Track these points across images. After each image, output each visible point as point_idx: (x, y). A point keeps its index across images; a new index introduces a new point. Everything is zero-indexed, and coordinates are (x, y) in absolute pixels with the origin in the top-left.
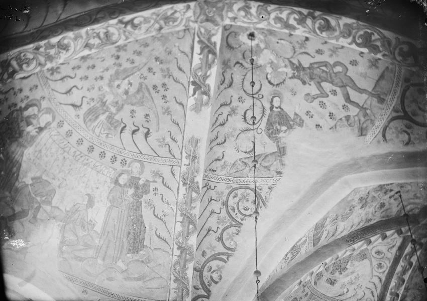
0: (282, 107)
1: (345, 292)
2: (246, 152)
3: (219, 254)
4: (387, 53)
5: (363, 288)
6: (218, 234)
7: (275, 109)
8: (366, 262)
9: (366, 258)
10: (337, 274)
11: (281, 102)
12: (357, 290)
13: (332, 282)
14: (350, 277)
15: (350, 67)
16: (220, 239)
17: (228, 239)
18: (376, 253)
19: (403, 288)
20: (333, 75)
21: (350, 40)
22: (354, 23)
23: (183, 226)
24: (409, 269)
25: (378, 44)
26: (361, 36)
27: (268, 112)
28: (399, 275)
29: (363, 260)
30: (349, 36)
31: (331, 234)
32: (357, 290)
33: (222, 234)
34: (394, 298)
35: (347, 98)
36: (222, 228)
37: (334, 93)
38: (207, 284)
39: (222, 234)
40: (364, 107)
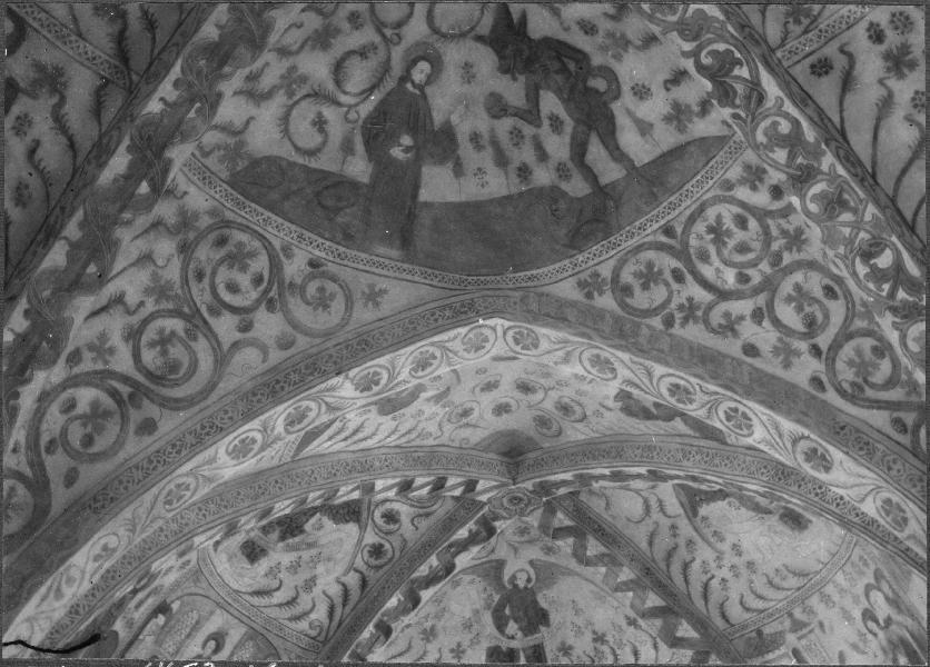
0: (428, 90)
2: (297, 149)
3: (112, 374)
4: (743, 115)
5: (317, 591)
6: (135, 320)
7: (409, 86)
8: (352, 528)
9: (358, 521)
10: (275, 535)
11: (430, 80)
14: (300, 553)
15: (628, 98)
16: (133, 335)
17: (152, 345)
18: (382, 517)
20: (581, 86)
21: (688, 47)
22: (717, 20)
23: (71, 257)
25: (739, 88)
26: (714, 53)
27: (390, 84)
29: (347, 521)
30: (694, 39)
33: (146, 322)
35: (579, 150)
36: (150, 307)
37: (556, 124)
38: (45, 439)
39: (146, 322)
40: (606, 190)
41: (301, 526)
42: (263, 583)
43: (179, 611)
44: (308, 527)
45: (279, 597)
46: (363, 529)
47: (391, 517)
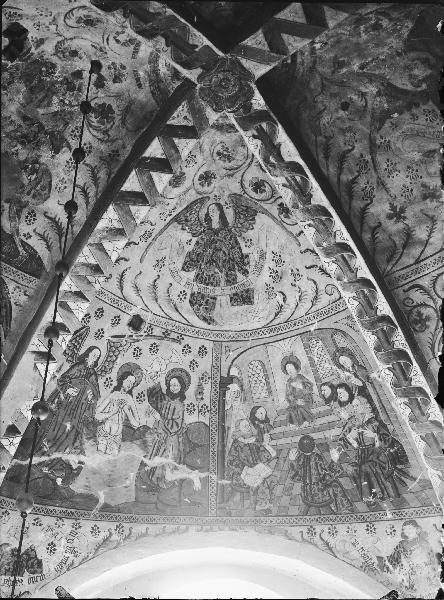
1: (282, 302)
5: (303, 271)
8: (261, 219)
9: (255, 213)
10: (240, 277)
12: (297, 283)
13: (244, 298)
14: (266, 268)
19: (338, 224)
24: (305, 181)
28: (301, 206)
29: (254, 219)
31: (52, 235)
32: (297, 283)
34: (343, 257)
44: (245, 251)
45: (292, 300)
47: (258, 186)
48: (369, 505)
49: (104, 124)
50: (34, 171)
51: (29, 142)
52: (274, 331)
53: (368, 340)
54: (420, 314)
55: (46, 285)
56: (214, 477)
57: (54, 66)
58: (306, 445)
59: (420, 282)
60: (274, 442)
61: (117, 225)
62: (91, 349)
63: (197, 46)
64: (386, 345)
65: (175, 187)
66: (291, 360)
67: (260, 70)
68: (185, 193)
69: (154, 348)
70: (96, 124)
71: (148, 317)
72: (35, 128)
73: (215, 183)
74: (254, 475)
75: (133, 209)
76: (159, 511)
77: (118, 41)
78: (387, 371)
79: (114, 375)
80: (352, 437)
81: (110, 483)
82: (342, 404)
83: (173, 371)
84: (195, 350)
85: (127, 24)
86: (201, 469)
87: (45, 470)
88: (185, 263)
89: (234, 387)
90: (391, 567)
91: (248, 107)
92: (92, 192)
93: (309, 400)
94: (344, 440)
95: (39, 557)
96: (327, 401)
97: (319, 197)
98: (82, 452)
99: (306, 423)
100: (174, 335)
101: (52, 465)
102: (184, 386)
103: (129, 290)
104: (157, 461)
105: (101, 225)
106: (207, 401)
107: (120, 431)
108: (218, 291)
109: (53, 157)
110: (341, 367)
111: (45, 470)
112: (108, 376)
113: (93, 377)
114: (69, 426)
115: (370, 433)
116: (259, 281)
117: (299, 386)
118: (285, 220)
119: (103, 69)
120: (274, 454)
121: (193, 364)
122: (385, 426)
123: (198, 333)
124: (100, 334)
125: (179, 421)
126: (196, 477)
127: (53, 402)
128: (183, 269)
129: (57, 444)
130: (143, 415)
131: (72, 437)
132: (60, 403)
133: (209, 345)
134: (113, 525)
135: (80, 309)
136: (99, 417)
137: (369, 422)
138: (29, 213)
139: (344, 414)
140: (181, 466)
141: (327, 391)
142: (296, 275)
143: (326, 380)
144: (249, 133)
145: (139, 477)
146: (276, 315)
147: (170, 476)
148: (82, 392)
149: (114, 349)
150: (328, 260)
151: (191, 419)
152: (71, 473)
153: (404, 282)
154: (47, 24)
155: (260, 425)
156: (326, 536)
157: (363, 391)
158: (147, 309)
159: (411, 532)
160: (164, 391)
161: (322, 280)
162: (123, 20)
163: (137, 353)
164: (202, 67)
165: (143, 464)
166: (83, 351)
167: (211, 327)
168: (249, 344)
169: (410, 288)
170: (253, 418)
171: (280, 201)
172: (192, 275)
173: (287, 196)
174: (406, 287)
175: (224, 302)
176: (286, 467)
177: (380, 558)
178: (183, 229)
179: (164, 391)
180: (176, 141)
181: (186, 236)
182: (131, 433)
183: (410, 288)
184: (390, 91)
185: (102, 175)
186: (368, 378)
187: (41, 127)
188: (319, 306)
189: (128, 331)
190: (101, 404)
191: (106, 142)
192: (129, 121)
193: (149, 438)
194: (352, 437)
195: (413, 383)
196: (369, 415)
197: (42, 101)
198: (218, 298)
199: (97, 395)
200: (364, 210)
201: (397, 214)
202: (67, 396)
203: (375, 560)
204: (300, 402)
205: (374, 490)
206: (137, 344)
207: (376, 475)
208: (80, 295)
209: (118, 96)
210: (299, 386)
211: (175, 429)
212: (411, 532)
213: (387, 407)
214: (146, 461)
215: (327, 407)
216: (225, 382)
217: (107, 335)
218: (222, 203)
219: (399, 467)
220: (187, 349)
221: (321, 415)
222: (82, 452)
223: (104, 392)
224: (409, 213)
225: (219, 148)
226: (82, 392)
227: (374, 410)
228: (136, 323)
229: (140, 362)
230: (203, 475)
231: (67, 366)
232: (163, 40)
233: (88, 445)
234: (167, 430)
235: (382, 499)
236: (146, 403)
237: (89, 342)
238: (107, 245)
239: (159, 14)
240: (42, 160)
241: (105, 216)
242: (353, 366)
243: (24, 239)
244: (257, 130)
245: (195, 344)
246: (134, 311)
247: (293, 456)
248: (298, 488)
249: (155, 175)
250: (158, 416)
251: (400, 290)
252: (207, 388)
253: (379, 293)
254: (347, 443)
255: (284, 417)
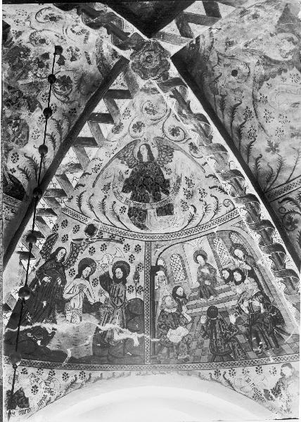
1: (193, 213)
5: (208, 191)
8: (177, 154)
9: (173, 150)
10: (163, 195)
12: (203, 199)
13: (167, 210)
14: (181, 189)
19: (231, 156)
24: (208, 126)
28: (205, 145)
29: (172, 155)
31: (30, 169)
32: (203, 199)
34: (235, 179)
41: (165, 180)
42: (187, 215)
43: (165, 263)
44: (166, 177)
45: (200, 211)
46: (180, 149)
47: (174, 131)
48: (257, 353)
49: (65, 90)
50: (16, 125)
51: (13, 104)
52: (187, 233)
53: (254, 237)
54: (290, 218)
55: (27, 205)
56: (148, 337)
57: (28, 50)
58: (212, 312)
59: (290, 196)
60: (190, 311)
61: (76, 161)
62: (59, 249)
63: (129, 34)
64: (267, 241)
65: (116, 133)
66: (200, 253)
67: (173, 49)
68: (124, 137)
69: (104, 248)
70: (59, 91)
71: (99, 226)
72: (16, 95)
73: (144, 130)
74: (176, 335)
75: (87, 149)
76: (111, 362)
77: (73, 32)
78: (268, 259)
79: (76, 267)
80: (244, 306)
81: (75, 342)
82: (237, 283)
83: (118, 262)
84: (133, 247)
85: (80, 19)
86: (137, 331)
87: (29, 335)
88: (124, 187)
89: (160, 273)
90: (274, 396)
91: (166, 76)
92: (57, 138)
93: (214, 280)
94: (239, 308)
95: (26, 396)
96: (227, 281)
97: (218, 138)
98: (55, 322)
99: (212, 297)
100: (117, 238)
101: (34, 331)
102: (126, 273)
103: (85, 207)
104: (108, 327)
105: (65, 161)
106: (142, 283)
107: (81, 306)
108: (148, 206)
109: (30, 114)
110: (236, 257)
111: (29, 335)
112: (72, 268)
113: (61, 269)
114: (45, 303)
115: (256, 303)
116: (177, 198)
117: (206, 271)
118: (195, 155)
119: (64, 51)
120: (189, 319)
121: (132, 256)
122: (267, 298)
123: (134, 237)
124: (65, 239)
125: (123, 298)
126: (135, 337)
127: (33, 287)
128: (123, 191)
129: (37, 318)
130: (97, 295)
131: (47, 311)
132: (38, 287)
133: (142, 244)
134: (78, 373)
135: (51, 221)
136: (66, 296)
137: (256, 295)
138: (14, 155)
139: (239, 290)
140: (124, 330)
141: (226, 274)
142: (203, 193)
143: (225, 267)
144: (168, 94)
145: (94, 338)
146: (189, 222)
147: (117, 337)
148: (54, 280)
149: (76, 249)
150: (224, 182)
151: (131, 296)
152: (47, 337)
153: (280, 196)
154: (24, 21)
155: (180, 300)
156: (227, 376)
157: (252, 274)
158: (98, 220)
159: (287, 371)
160: (111, 277)
161: (222, 197)
162: (77, 16)
163: (92, 251)
164: (133, 48)
165: (98, 329)
166: (53, 251)
167: (143, 231)
168: (170, 243)
169: (284, 200)
170: (174, 295)
171: (190, 141)
172: (129, 195)
173: (196, 138)
174: (281, 199)
175: (152, 215)
176: (199, 328)
177: (266, 391)
178: (122, 163)
179: (111, 277)
180: (116, 100)
181: (124, 168)
182: (89, 308)
183: (284, 200)
184: (267, 61)
185: (65, 126)
186: (255, 264)
187: (20, 93)
188: (219, 214)
189: (85, 236)
190: (68, 288)
191: (67, 103)
192: (83, 87)
193: (102, 311)
194: (244, 306)
195: (287, 267)
196: (256, 291)
197: (21, 75)
198: (148, 211)
199: (64, 282)
200: (249, 147)
201: (273, 148)
202: (44, 283)
203: (262, 392)
204: (207, 283)
205: (261, 343)
206: (91, 245)
207: (262, 333)
208: (50, 211)
209: (74, 70)
210: (206, 271)
211: (120, 304)
212: (287, 371)
213: (269, 284)
214: (100, 327)
215: (226, 286)
216: (154, 270)
217: (70, 240)
218: (149, 143)
219: (278, 326)
220: (127, 247)
221: (222, 291)
222: (55, 322)
223: (69, 279)
224: (281, 147)
225: (146, 105)
226: (54, 280)
227: (260, 286)
228: (91, 230)
229: (94, 257)
230: (140, 336)
231: (43, 262)
232: (105, 30)
233: (58, 316)
234: (113, 305)
235: (267, 349)
236: (99, 287)
237: (58, 244)
238: (69, 176)
239: (102, 11)
240: (22, 117)
241: (67, 154)
242: (244, 256)
243: (10, 173)
244: (173, 92)
245: (133, 244)
246: (90, 221)
247: (203, 321)
248: (207, 343)
249: (102, 125)
250: (107, 295)
251: (277, 202)
252: (142, 274)
253: (262, 205)
254: (241, 311)
255: (196, 294)
